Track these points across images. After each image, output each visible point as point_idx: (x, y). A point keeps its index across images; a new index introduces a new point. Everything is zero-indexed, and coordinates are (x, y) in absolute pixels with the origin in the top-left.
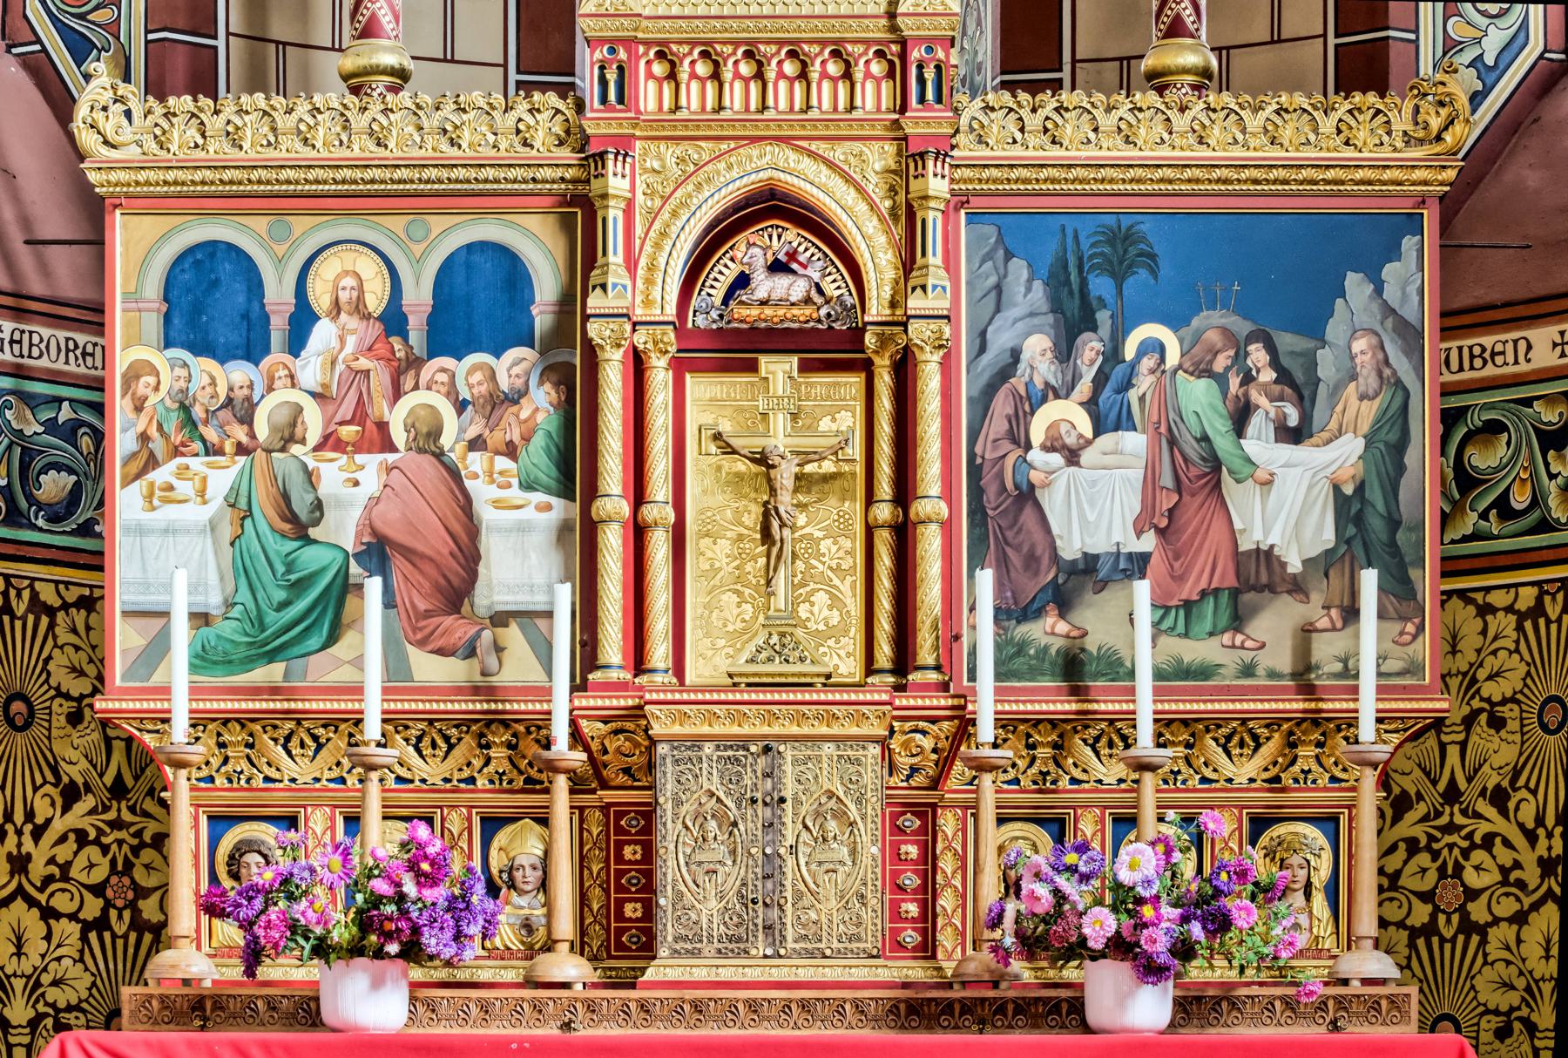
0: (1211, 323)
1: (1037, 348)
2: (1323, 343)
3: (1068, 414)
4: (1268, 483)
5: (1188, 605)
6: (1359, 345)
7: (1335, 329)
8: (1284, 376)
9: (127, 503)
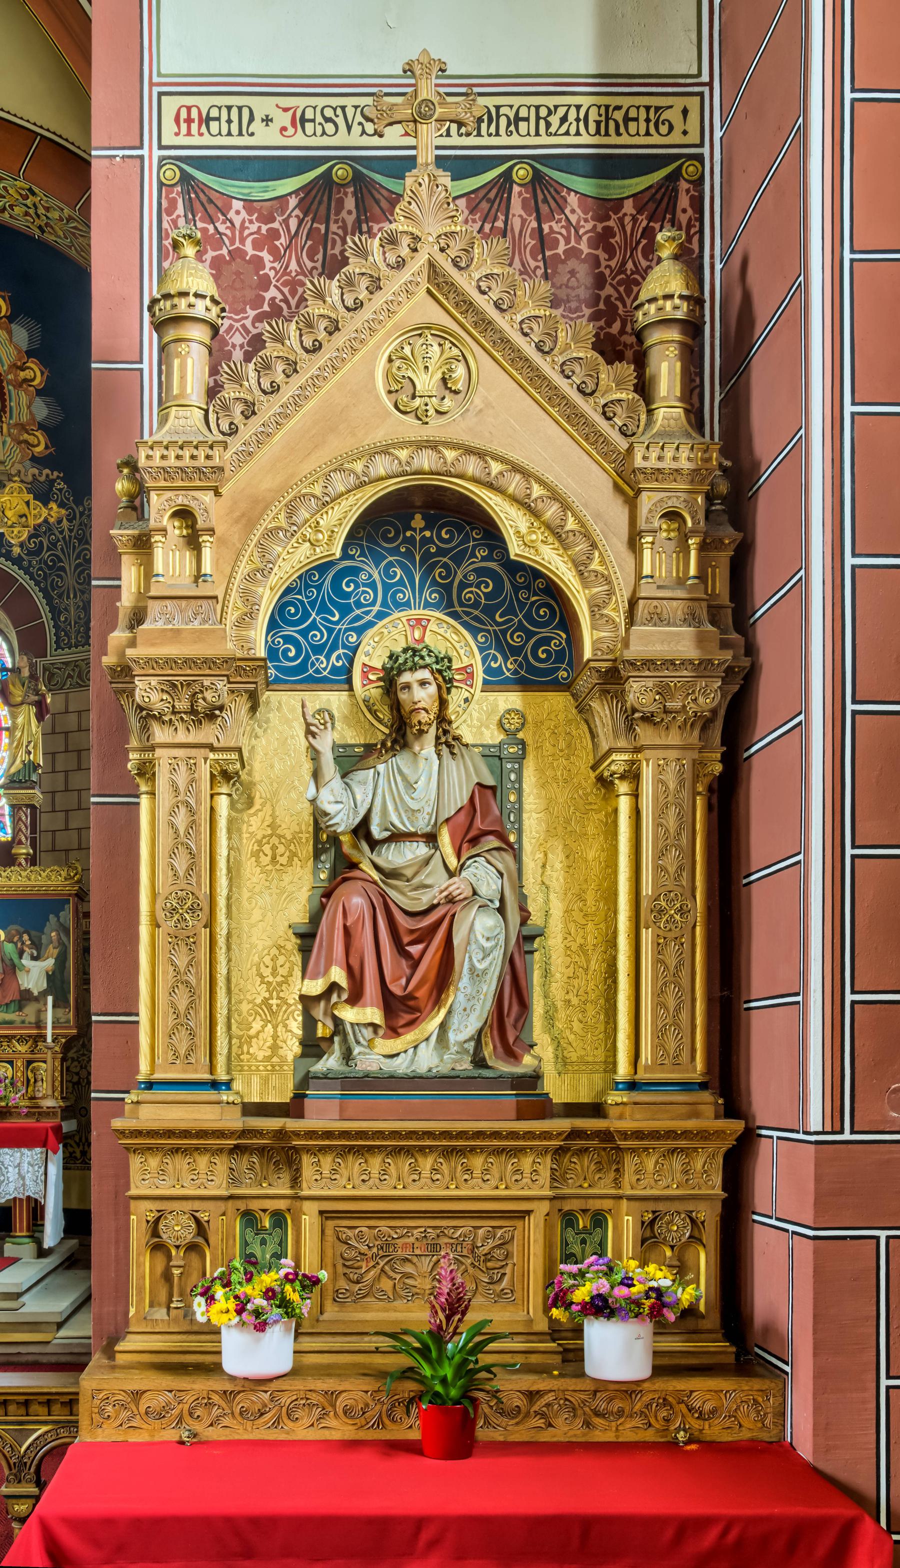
0: (13, 928)
2: (43, 933)
4: (28, 971)
5: (7, 1005)
6: (53, 934)
7: (46, 930)
8: (33, 943)
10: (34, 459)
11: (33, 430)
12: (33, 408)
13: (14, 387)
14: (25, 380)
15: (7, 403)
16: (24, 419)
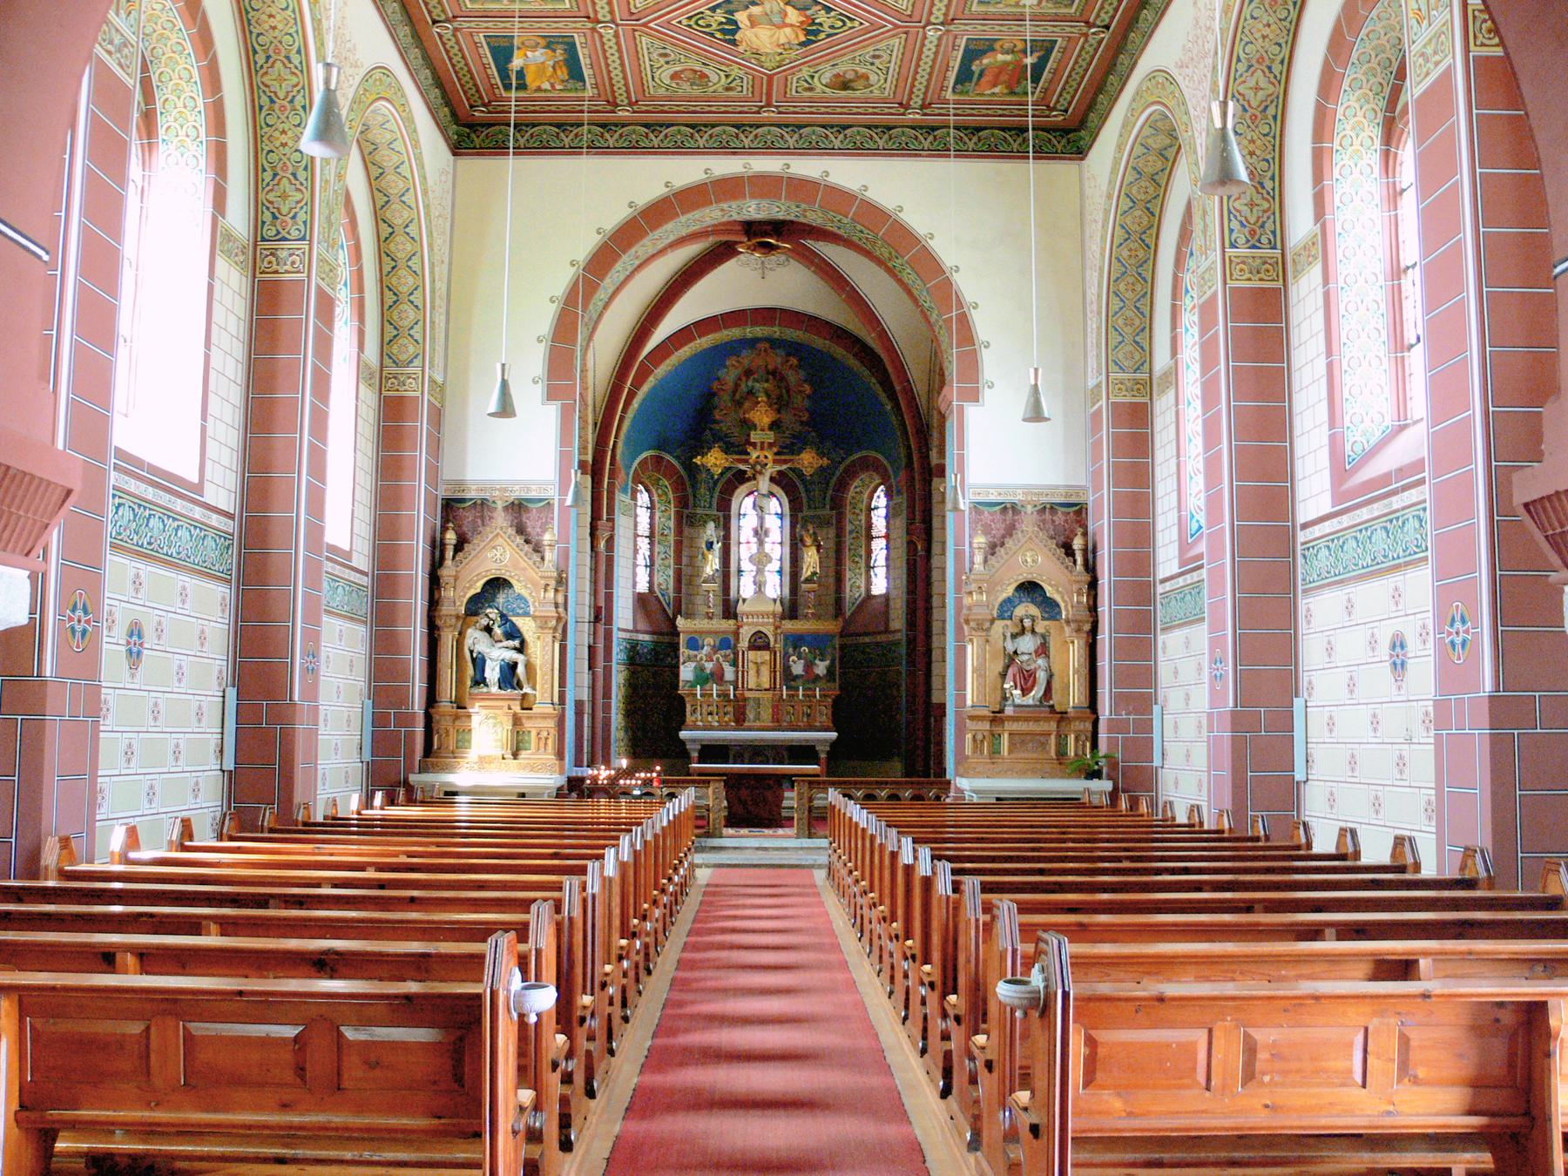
1: (791, 650)
3: (795, 658)
9: (682, 667)
10: (802, 422)
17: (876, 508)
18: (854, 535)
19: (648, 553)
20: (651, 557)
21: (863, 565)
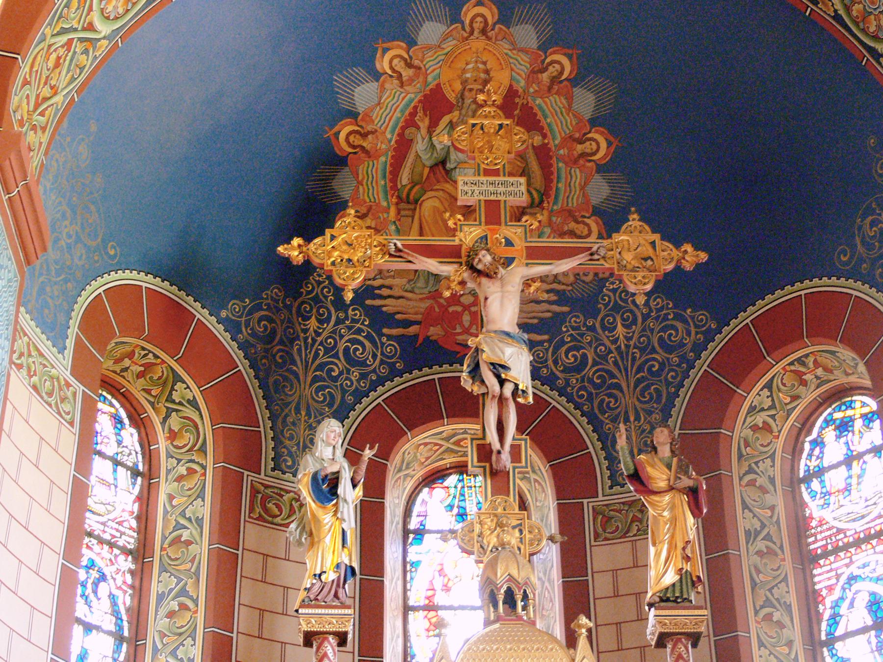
11: (585, 217)
12: (588, 189)
13: (566, 163)
14: (583, 155)
15: (554, 185)
16: (574, 203)
17: (820, 472)
18: (761, 545)
19: (125, 600)
20: (138, 616)
21: (795, 632)
